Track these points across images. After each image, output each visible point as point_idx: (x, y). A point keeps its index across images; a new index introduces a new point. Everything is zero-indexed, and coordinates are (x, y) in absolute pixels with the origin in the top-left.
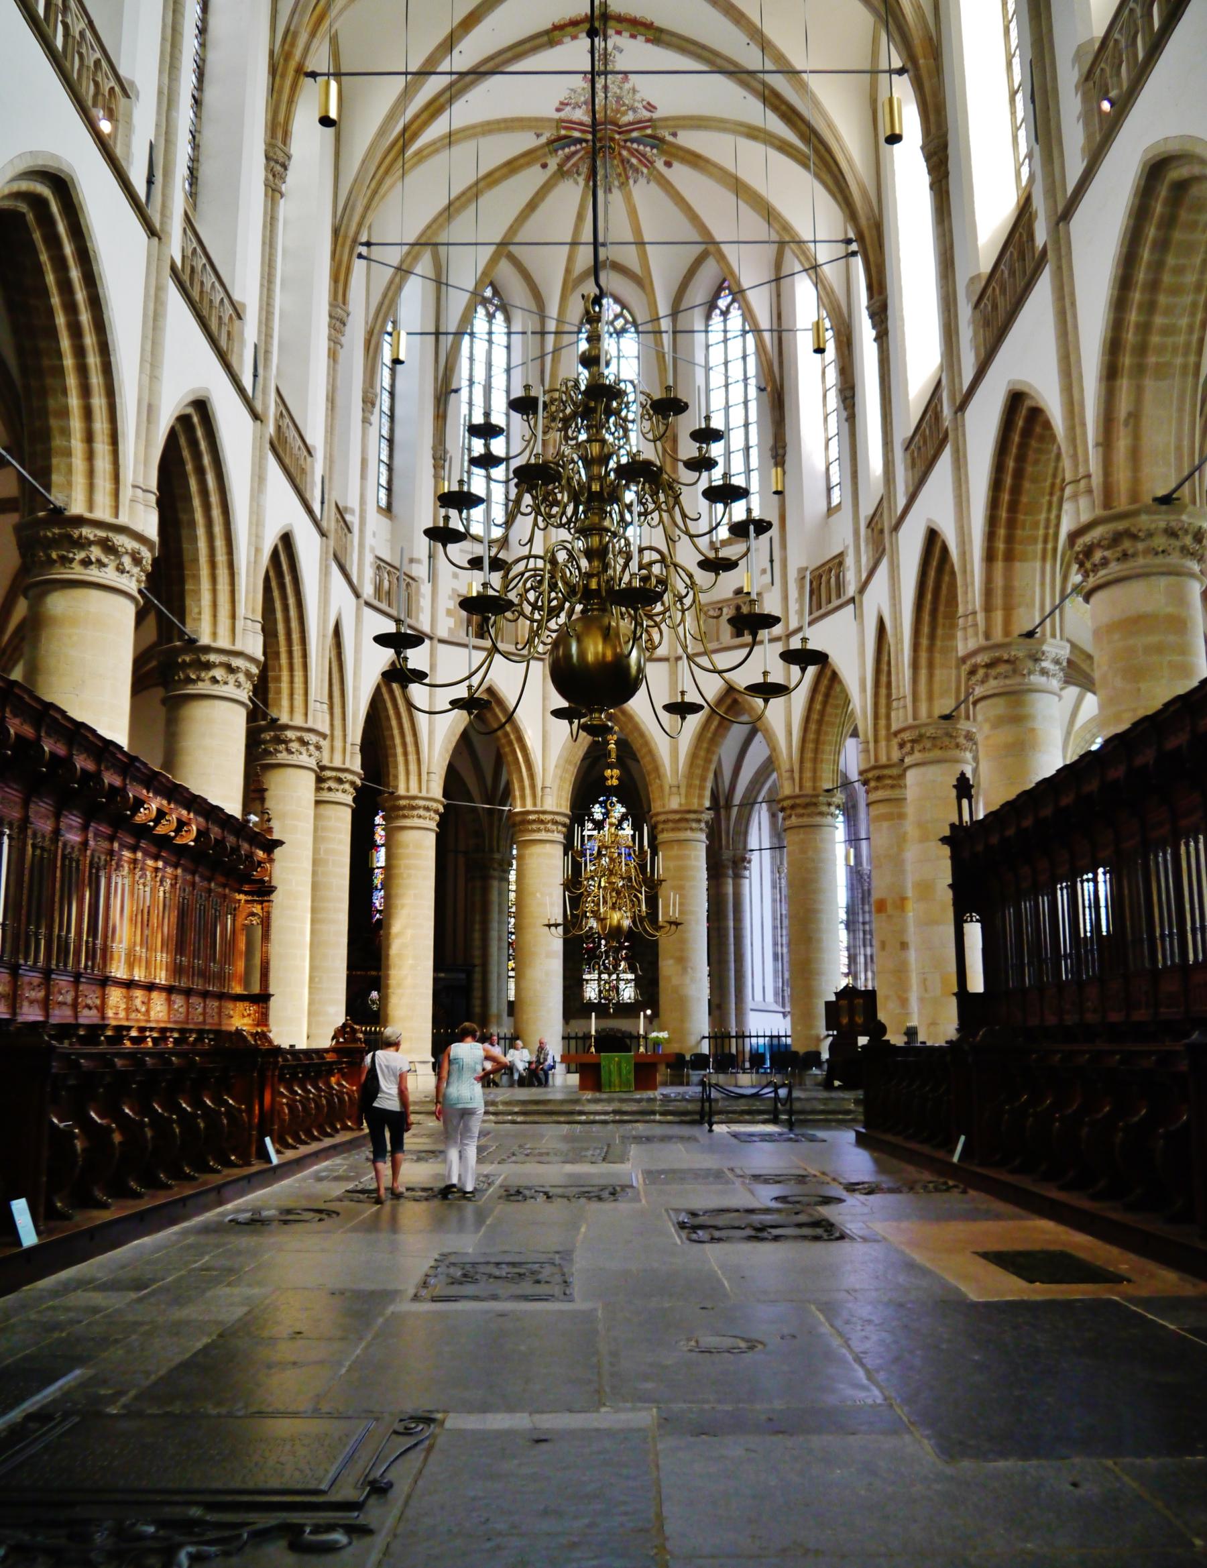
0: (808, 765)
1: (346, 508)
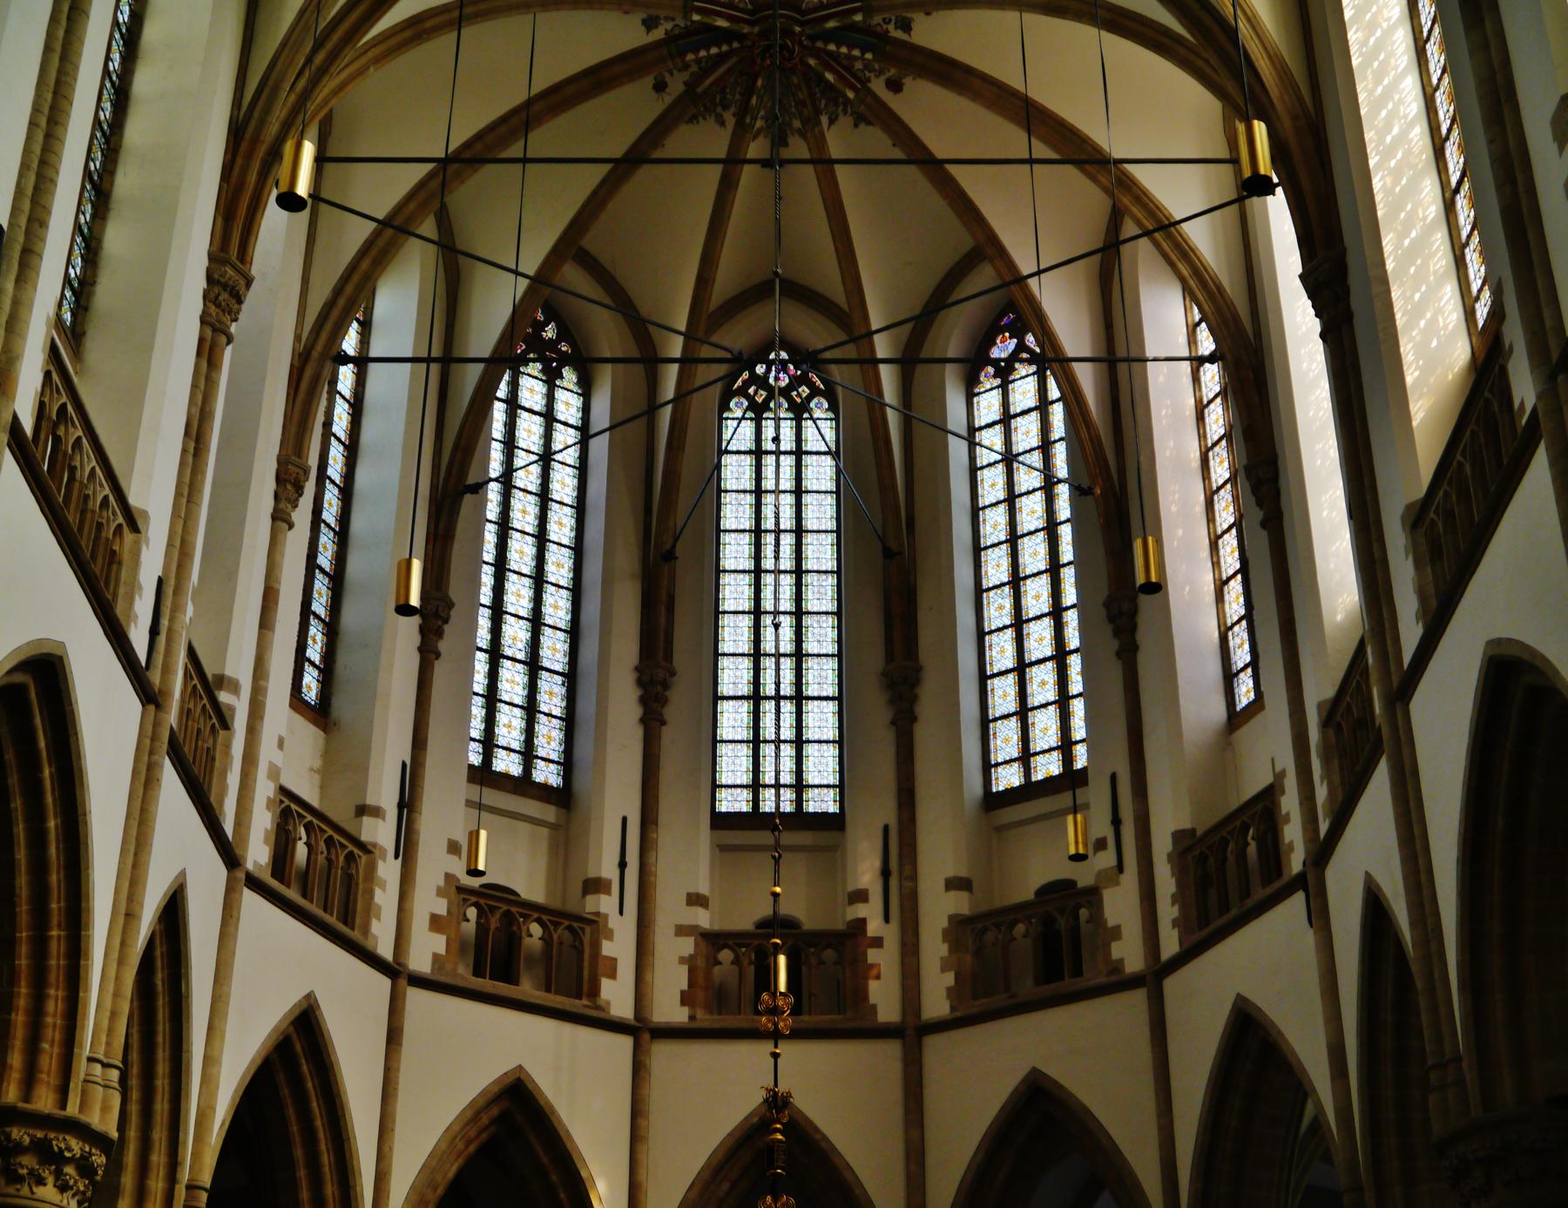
1: (221, 681)
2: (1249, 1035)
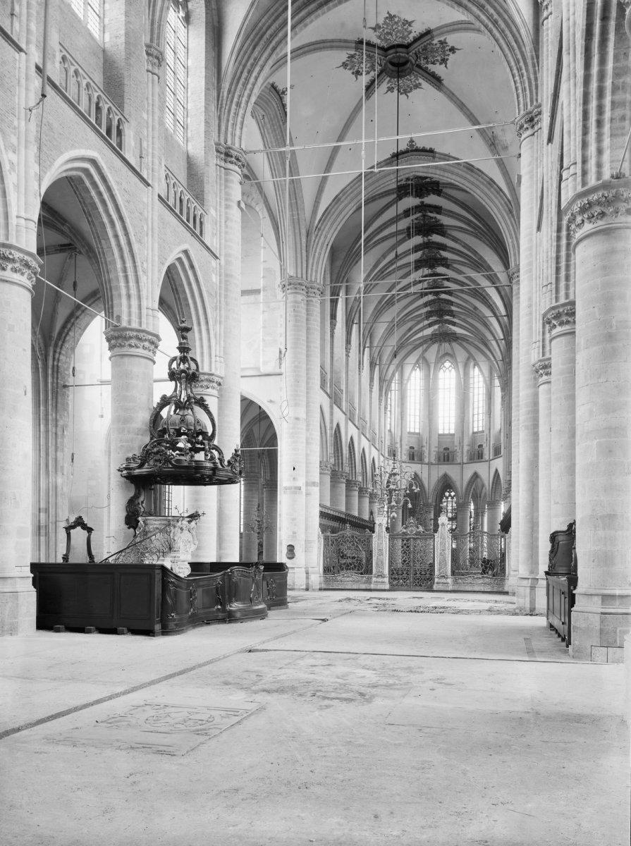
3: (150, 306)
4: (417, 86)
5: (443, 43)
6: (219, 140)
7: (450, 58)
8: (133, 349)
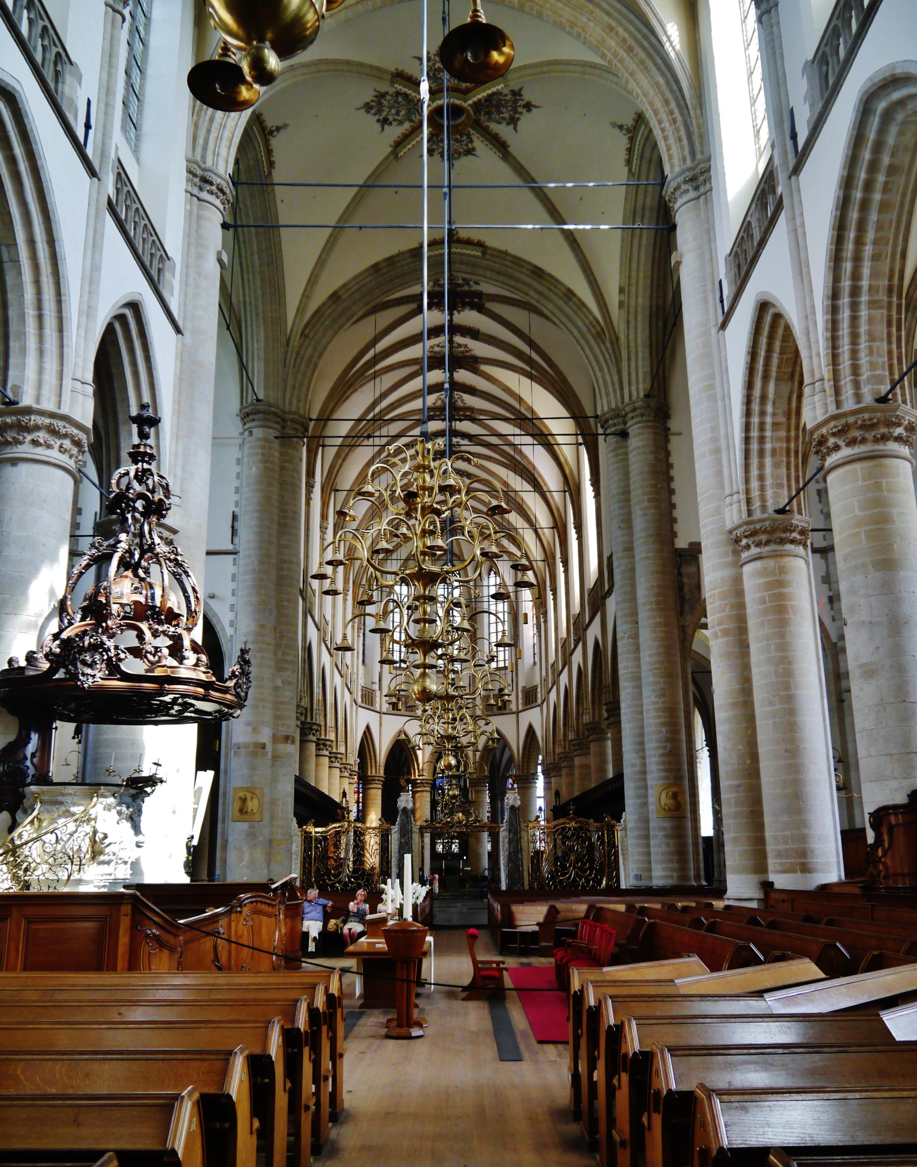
0: (525, 764)
2: (531, 729)
3: (79, 376)
4: (470, 152)
5: (517, 94)
6: (194, 156)
7: (522, 117)
8: (39, 450)
